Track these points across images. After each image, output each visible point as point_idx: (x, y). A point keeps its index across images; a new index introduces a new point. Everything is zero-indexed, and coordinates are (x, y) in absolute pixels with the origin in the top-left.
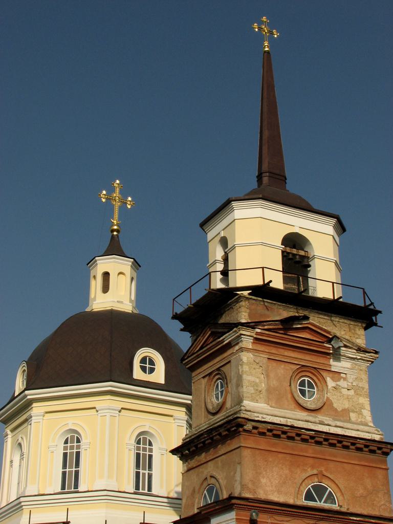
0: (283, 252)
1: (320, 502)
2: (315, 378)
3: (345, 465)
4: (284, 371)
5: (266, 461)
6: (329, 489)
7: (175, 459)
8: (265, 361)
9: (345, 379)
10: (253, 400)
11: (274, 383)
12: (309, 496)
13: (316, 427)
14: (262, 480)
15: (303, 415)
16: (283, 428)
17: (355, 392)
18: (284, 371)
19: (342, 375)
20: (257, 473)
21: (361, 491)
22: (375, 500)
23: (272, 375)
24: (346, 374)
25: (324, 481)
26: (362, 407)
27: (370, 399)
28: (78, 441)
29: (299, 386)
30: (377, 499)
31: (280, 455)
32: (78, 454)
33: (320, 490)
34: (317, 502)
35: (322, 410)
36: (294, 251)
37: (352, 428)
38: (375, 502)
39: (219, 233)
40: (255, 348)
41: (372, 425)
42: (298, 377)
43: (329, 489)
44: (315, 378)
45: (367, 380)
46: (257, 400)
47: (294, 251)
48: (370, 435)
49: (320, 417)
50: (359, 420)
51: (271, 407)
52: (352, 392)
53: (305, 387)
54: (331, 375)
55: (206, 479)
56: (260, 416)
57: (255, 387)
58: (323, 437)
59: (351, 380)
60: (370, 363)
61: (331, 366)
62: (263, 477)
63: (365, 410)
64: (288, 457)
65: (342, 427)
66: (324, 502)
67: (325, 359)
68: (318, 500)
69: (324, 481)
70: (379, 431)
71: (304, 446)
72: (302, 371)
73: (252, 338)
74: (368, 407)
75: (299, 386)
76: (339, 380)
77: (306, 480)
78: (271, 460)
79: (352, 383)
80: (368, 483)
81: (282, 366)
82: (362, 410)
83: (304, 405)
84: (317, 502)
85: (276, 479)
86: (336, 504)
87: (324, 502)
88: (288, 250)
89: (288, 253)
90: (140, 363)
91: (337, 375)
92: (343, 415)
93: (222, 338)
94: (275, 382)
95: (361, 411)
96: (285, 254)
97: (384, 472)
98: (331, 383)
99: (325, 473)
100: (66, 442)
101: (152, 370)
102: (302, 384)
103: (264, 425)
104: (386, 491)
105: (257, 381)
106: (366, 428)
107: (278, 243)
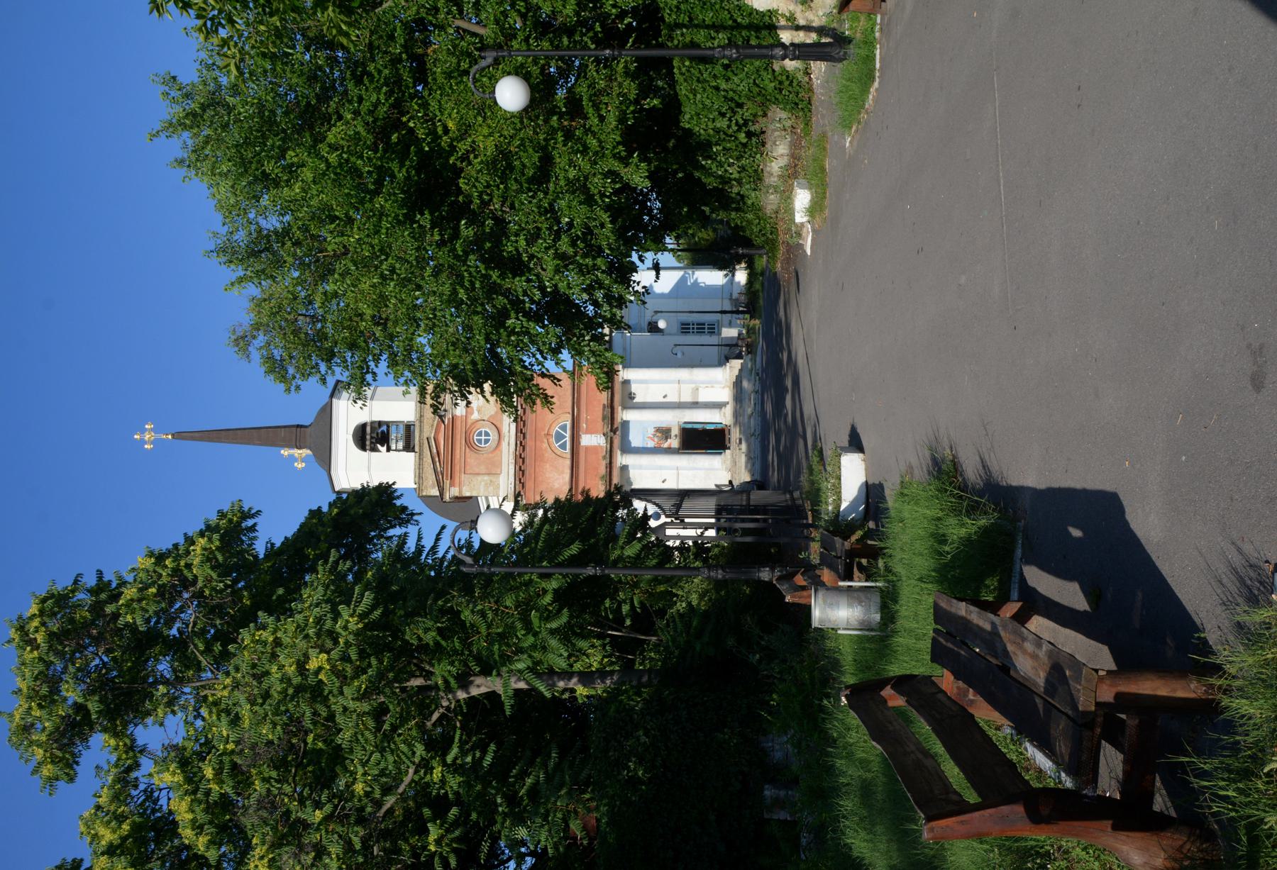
10: (499, 488)
11: (483, 469)
15: (504, 444)
18: (472, 458)
23: (477, 470)
33: (559, 437)
47: (368, 437)
71: (528, 449)
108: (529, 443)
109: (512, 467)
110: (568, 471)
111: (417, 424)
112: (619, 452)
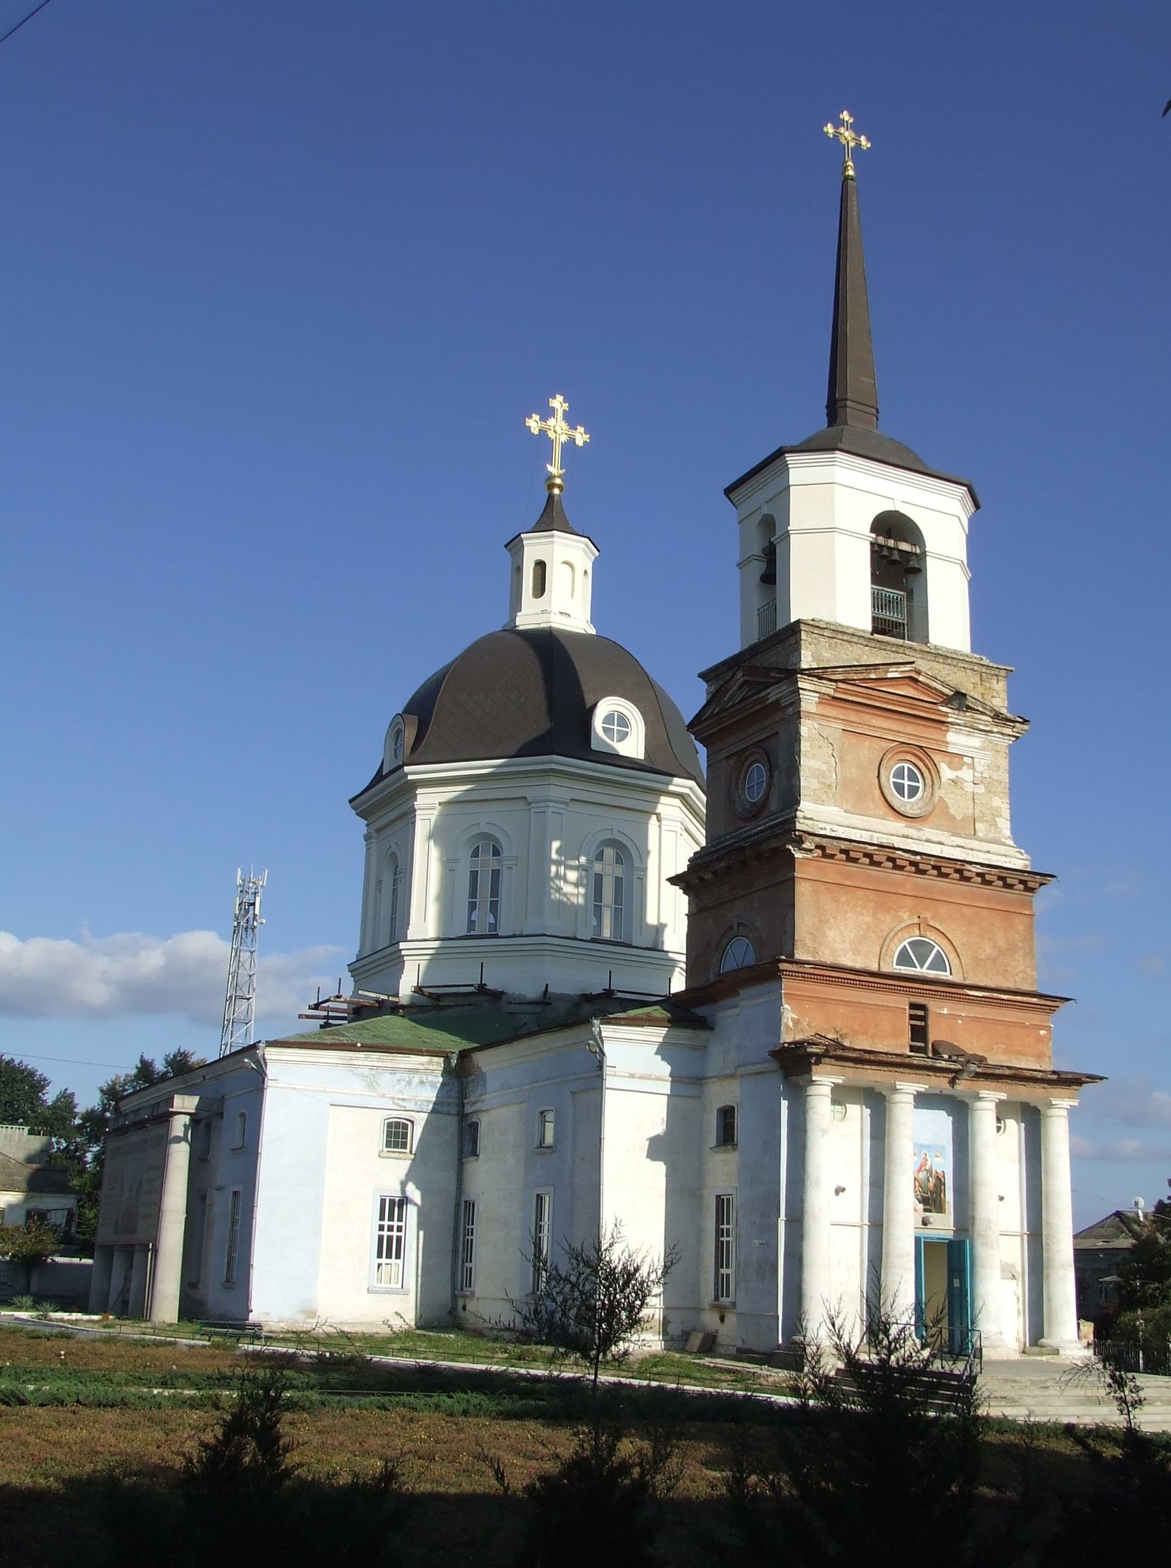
0: (872, 544)
1: (922, 967)
2: (920, 764)
3: (965, 909)
4: (868, 751)
5: (835, 901)
6: (937, 948)
7: (677, 891)
8: (839, 733)
9: (972, 767)
10: (815, 802)
12: (904, 959)
13: (921, 846)
14: (828, 933)
15: (899, 826)
16: (866, 848)
17: (986, 788)
18: (868, 751)
19: (965, 759)
20: (820, 921)
21: (987, 950)
22: (1009, 964)
24: (972, 758)
25: (928, 934)
26: (997, 813)
27: (1010, 800)
28: (496, 852)
29: (894, 777)
30: (1012, 963)
31: (860, 893)
32: (496, 874)
34: (916, 967)
35: (930, 819)
36: (891, 543)
37: (978, 848)
38: (1009, 968)
39: (760, 507)
40: (821, 712)
41: (1011, 843)
42: (892, 762)
43: (937, 948)
44: (920, 764)
45: (1007, 767)
46: (823, 801)
47: (891, 543)
48: (1007, 860)
49: (928, 832)
50: (991, 835)
51: (846, 812)
52: (981, 789)
53: (904, 779)
54: (947, 759)
55: (731, 927)
56: (828, 827)
57: (822, 780)
58: (932, 863)
59: (979, 768)
60: (1014, 739)
61: (947, 743)
62: (830, 928)
63: (1001, 819)
64: (872, 896)
65: (963, 847)
66: (928, 969)
67: (938, 731)
68: (917, 965)
69: (928, 934)
70: (1021, 854)
72: (915, 755)
73: (818, 695)
74: (1006, 813)
75: (894, 777)
76: (961, 769)
77: (900, 933)
78: (843, 899)
79: (982, 773)
80: (1001, 938)
81: (867, 744)
82: (997, 819)
83: (901, 810)
84: (916, 967)
85: (851, 931)
86: (946, 971)
87: (928, 969)
88: (881, 540)
89: (880, 546)
90: (603, 723)
91: (956, 759)
92: (967, 827)
93: (763, 694)
94: (853, 770)
95: (995, 821)
96: (876, 548)
97: (1026, 920)
98: (947, 773)
99: (932, 923)
100: (475, 854)
101: (623, 736)
102: (899, 774)
103: (835, 842)
104: (1028, 951)
105: (825, 768)
106: (1002, 849)
107: (864, 526)
108: (908, 881)
109: (865, 837)
110: (858, 964)
111: (924, 648)
112: (922, 1088)
